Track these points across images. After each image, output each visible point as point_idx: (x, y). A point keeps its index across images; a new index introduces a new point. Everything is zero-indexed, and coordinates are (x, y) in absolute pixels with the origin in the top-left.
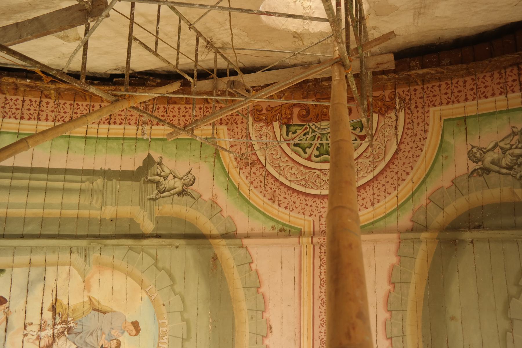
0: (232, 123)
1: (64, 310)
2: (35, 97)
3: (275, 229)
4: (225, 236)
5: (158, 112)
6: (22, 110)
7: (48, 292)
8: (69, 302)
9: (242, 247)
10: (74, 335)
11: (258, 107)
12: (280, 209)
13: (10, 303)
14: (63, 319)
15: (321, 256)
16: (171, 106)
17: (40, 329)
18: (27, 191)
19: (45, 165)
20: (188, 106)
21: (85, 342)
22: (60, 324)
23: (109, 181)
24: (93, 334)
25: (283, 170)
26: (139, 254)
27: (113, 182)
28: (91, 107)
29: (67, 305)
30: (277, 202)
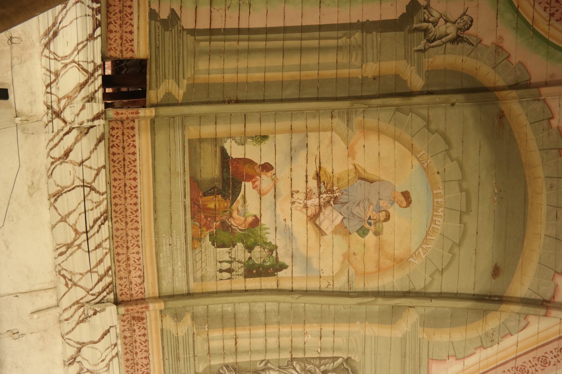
1: (329, 179)
7: (312, 160)
8: (333, 170)
9: (539, 100)
10: (340, 205)
13: (276, 170)
14: (328, 188)
17: (306, 197)
18: (282, 52)
19: (297, 23)
21: (352, 212)
22: (326, 192)
23: (369, 34)
27: (373, 35)
29: (332, 174)
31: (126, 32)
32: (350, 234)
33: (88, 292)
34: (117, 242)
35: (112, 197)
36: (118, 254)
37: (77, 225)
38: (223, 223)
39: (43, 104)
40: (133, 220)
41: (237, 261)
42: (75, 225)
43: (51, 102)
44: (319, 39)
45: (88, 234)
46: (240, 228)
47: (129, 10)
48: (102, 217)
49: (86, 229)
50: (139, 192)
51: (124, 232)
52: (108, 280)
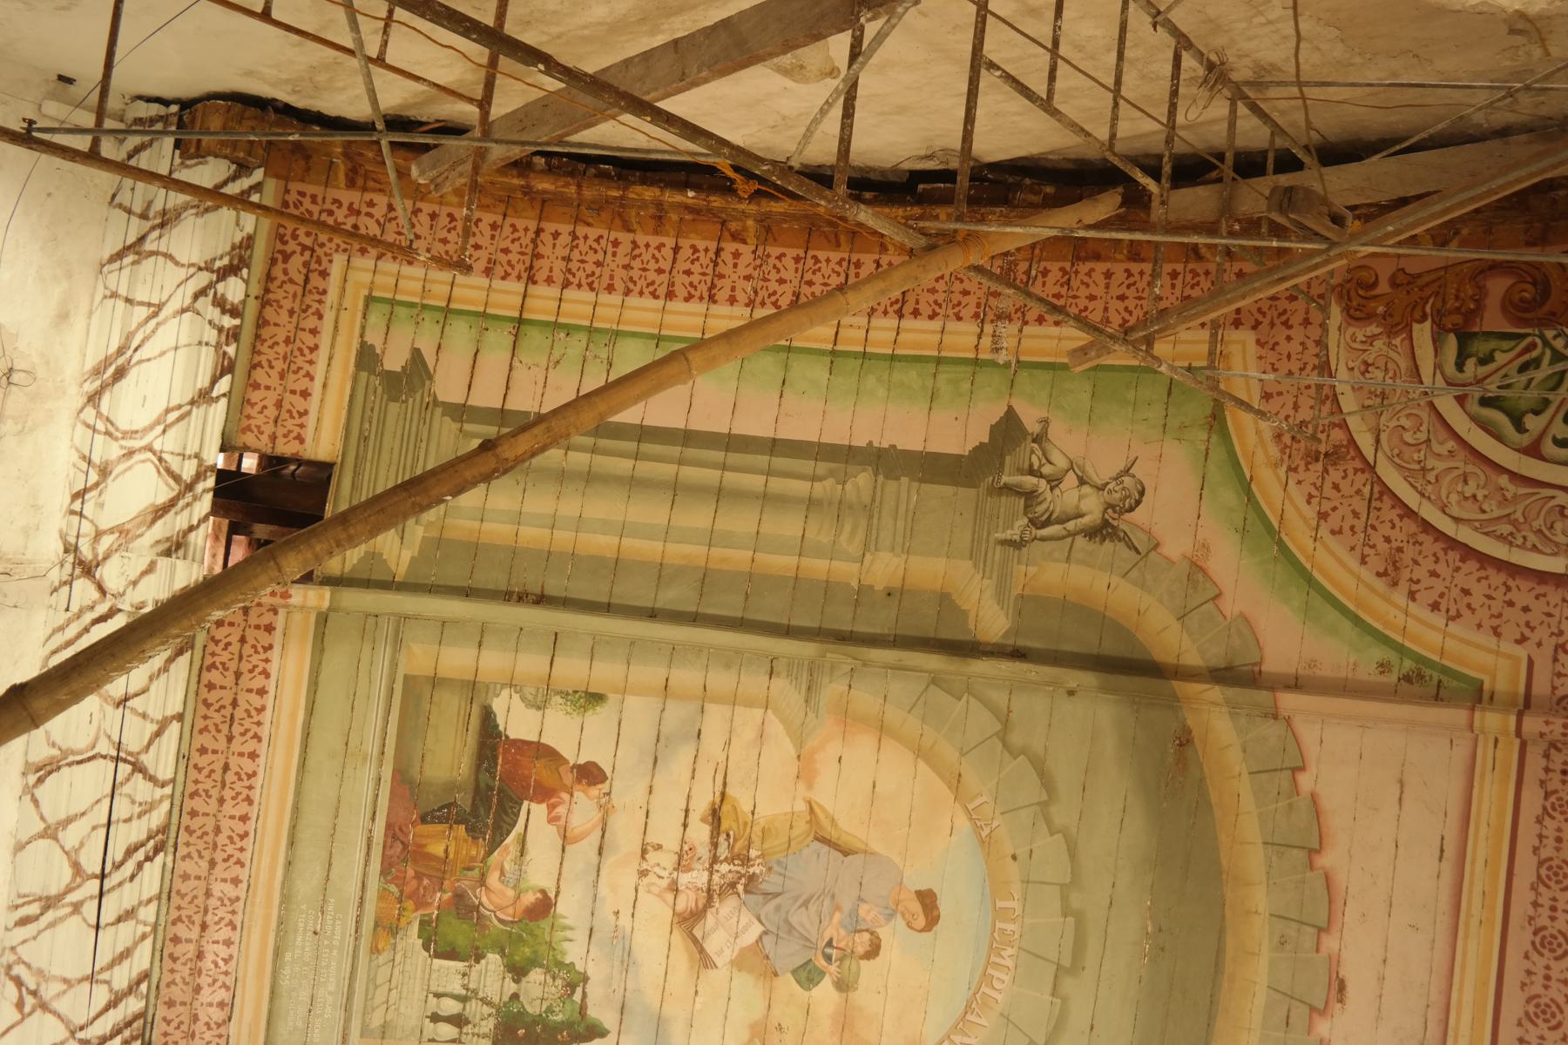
0: (1272, 325)
2: (705, 238)
3: (1390, 671)
4: (1224, 675)
5: (1044, 284)
6: (670, 273)
7: (705, 772)
9: (1275, 717)
10: (760, 898)
11: (1364, 273)
12: (1413, 607)
14: (736, 850)
15: (1548, 783)
16: (1084, 268)
20: (1135, 267)
21: (787, 921)
22: (728, 860)
24: (810, 906)
25: (1433, 481)
26: (959, 699)
28: (852, 267)
30: (1404, 586)
31: (293, 392)
32: (776, 974)
33: (73, 1033)
34: (179, 908)
35: (187, 794)
36: (176, 940)
37: (83, 851)
38: (459, 897)
39: (57, 536)
40: (230, 856)
41: (481, 1000)
42: (77, 851)
43: (78, 537)
44: (769, 473)
45: (106, 881)
46: (502, 916)
47: (309, 340)
48: (152, 843)
49: (103, 869)
50: (257, 791)
51: (202, 884)
52: (133, 1005)
